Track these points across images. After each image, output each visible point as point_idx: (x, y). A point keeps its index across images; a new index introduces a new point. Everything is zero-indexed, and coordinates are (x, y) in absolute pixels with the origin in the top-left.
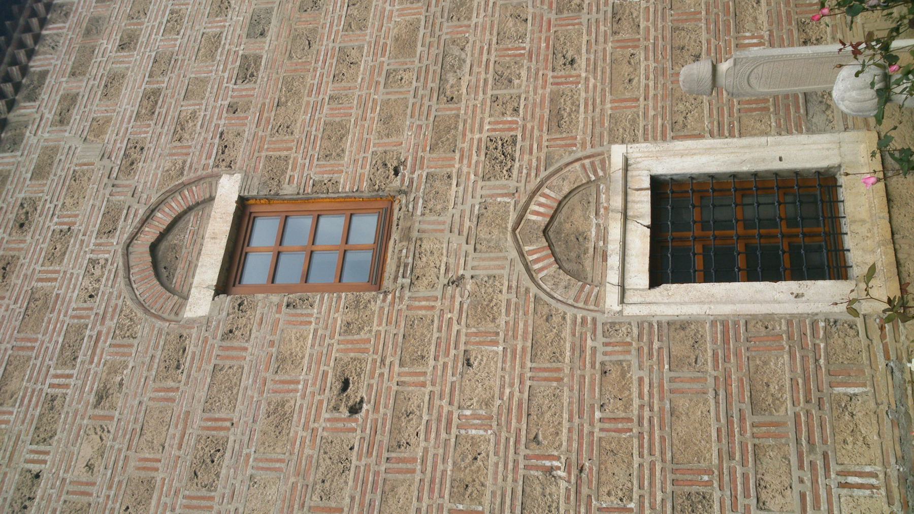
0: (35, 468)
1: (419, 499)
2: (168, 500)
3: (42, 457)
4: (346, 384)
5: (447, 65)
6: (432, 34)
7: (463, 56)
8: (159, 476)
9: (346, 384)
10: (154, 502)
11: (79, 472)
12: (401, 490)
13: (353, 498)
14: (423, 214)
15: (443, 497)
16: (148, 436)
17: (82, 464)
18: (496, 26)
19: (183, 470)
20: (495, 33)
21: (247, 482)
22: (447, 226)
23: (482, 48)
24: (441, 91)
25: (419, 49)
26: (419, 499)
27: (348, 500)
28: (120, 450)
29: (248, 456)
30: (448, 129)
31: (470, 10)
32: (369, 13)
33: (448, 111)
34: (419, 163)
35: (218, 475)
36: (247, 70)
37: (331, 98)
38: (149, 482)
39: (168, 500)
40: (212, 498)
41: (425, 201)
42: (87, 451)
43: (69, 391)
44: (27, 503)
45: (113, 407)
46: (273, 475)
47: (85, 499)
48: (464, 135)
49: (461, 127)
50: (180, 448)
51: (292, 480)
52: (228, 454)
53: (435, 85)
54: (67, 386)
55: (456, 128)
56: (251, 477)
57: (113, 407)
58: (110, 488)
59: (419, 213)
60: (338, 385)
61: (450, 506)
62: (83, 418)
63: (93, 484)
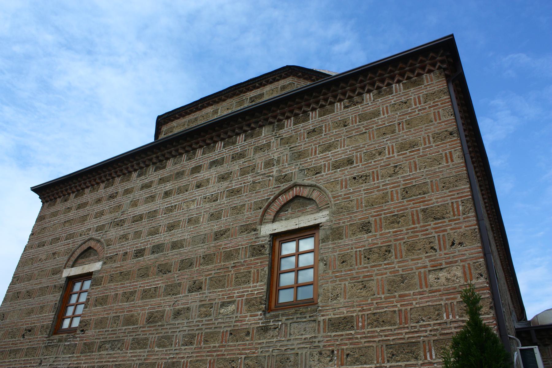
4: (30, 331)
5: (115, 343)
6: (129, 332)
7: (116, 349)
9: (30, 331)
14: (65, 345)
18: (123, 363)
20: (120, 363)
22: (57, 356)
23: (115, 358)
24: (104, 343)
25: (124, 328)
30: (89, 349)
31: (135, 348)
32: (149, 299)
33: (96, 347)
34: (82, 339)
36: (139, 253)
37: (117, 294)
41: (69, 345)
48: (85, 356)
49: (89, 354)
53: (108, 339)
55: (89, 352)
59: (66, 343)
60: (30, 328)
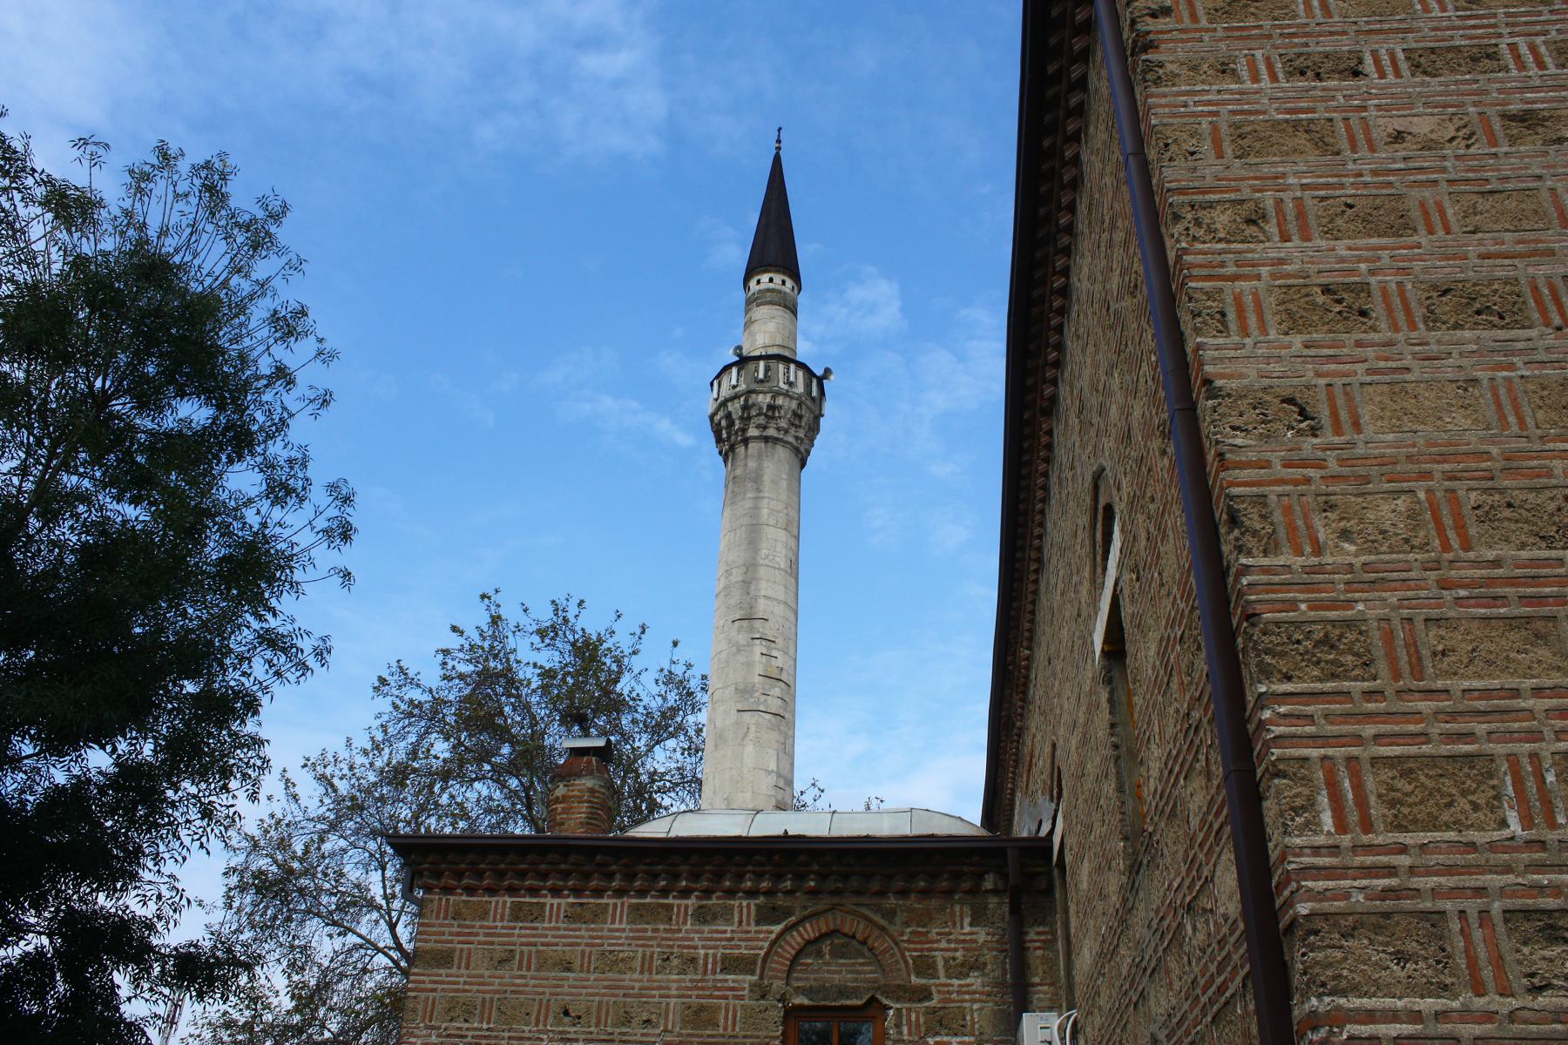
0: (1369, 65)
1: (1538, 691)
2: (1386, 261)
3: (1389, 70)
8: (1422, 238)
10: (1374, 241)
11: (1385, 125)
12: (1542, 652)
13: (1496, 563)
15: (1559, 740)
16: (1482, 205)
17: (1399, 124)
19: (1444, 271)
21: (1462, 376)
26: (1538, 691)
27: (1491, 555)
28: (1444, 170)
29: (1511, 367)
35: (1457, 326)
38: (1406, 226)
39: (1386, 261)
40: (1413, 326)
42: (1423, 126)
43: (1514, 73)
44: (1309, 73)
45: (1513, 141)
46: (1491, 414)
47: (1344, 145)
50: (1482, 256)
51: (1495, 450)
52: (1500, 334)
54: (1522, 66)
56: (1474, 381)
57: (1513, 141)
58: (1375, 173)
61: (1546, 754)
62: (1475, 104)
63: (1372, 149)
